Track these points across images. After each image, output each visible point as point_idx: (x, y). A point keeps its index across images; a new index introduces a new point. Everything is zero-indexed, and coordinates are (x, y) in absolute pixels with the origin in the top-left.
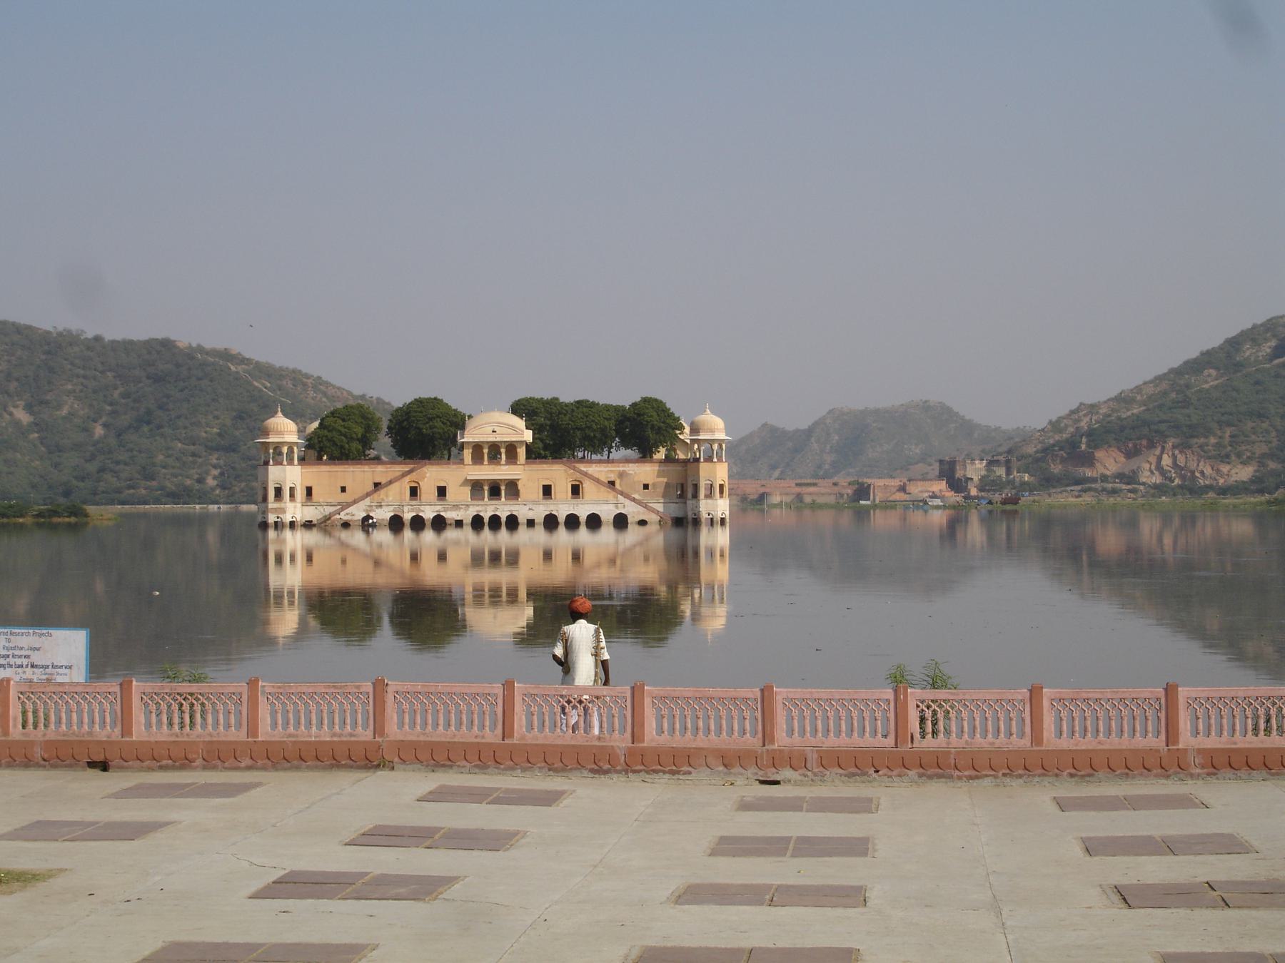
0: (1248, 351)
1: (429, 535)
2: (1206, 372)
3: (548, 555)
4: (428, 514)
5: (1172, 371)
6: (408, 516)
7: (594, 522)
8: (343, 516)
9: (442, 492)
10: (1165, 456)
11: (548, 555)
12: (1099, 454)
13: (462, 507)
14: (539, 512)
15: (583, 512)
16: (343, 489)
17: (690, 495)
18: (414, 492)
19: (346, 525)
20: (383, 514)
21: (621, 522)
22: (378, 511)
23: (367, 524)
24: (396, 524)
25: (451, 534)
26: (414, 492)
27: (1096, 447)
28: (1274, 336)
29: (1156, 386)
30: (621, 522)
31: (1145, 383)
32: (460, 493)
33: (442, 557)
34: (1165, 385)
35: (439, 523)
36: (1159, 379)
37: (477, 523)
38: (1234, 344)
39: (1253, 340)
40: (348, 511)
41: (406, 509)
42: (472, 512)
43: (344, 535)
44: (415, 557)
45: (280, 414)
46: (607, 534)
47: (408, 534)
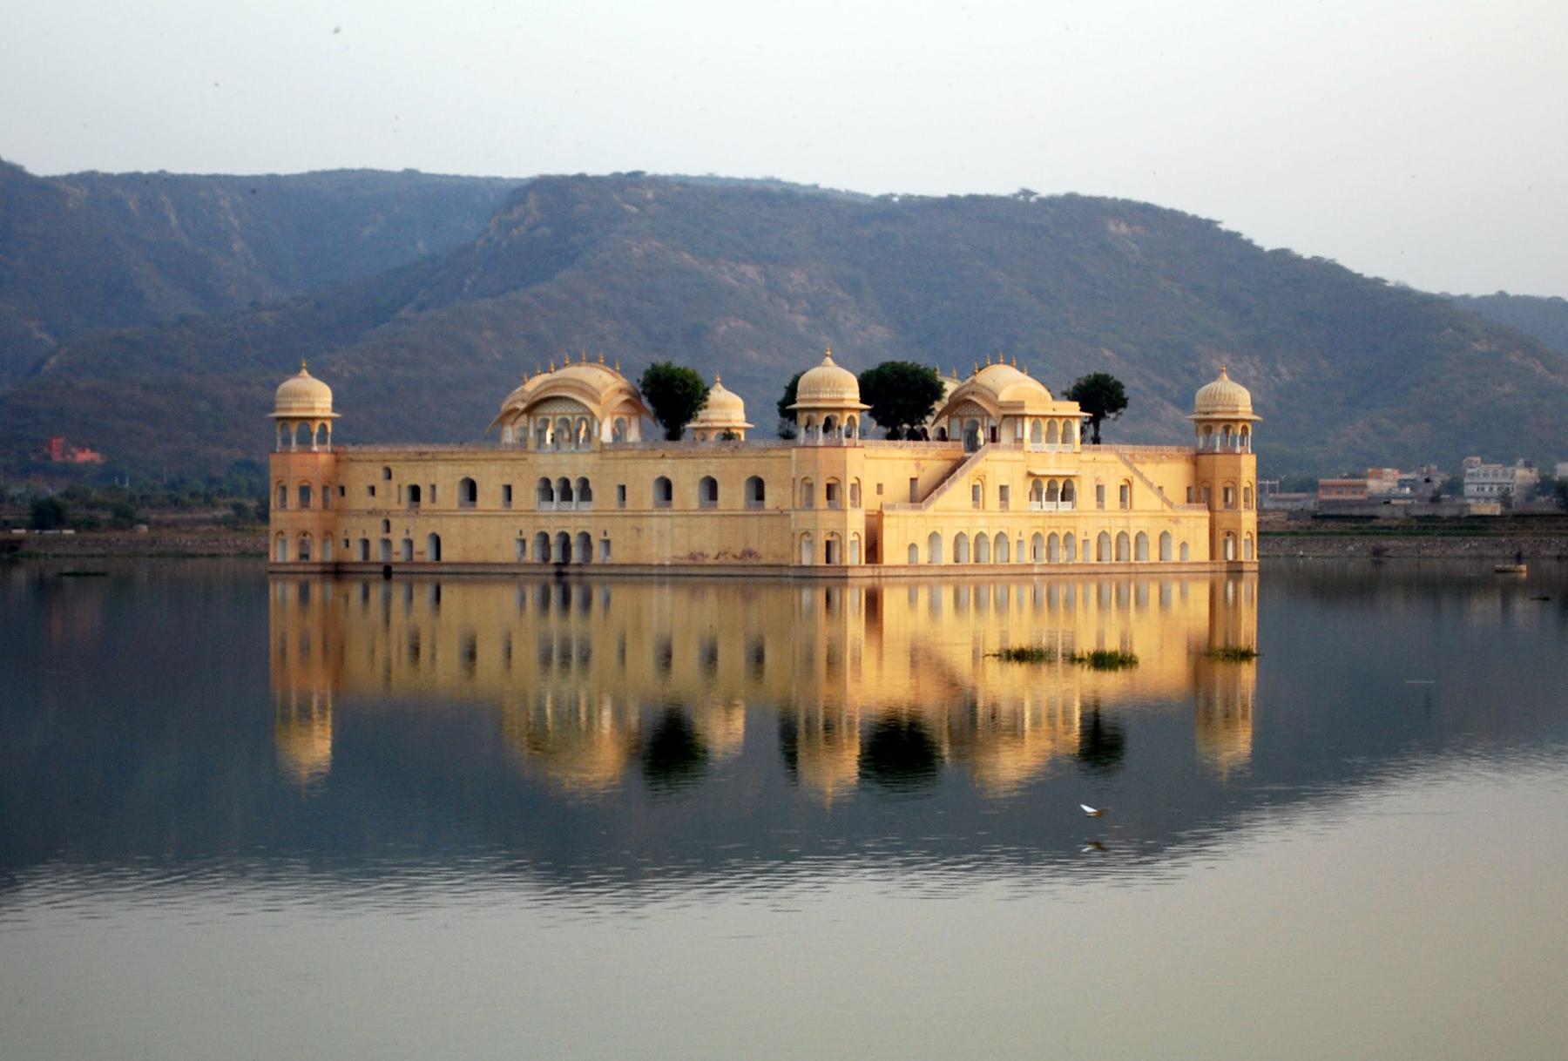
17: (1219, 503)
45: (829, 360)
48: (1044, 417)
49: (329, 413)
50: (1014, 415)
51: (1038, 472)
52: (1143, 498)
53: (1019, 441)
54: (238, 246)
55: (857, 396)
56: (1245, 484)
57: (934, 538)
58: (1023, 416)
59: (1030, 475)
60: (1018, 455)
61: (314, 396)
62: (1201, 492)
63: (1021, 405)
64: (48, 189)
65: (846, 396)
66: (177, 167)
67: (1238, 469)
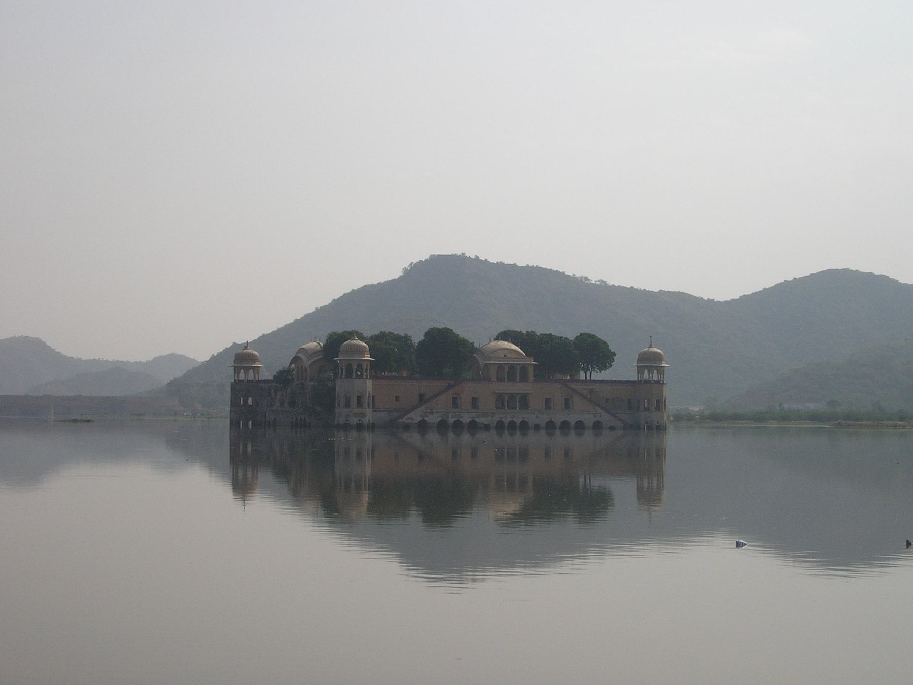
1: (466, 438)
3: (547, 454)
4: (466, 419)
5: (296, 321)
6: (451, 421)
7: (580, 426)
8: (404, 420)
11: (547, 454)
14: (543, 419)
15: (573, 419)
16: (397, 398)
18: (455, 401)
19: (407, 427)
20: (433, 419)
21: (597, 426)
22: (431, 416)
23: (423, 427)
24: (442, 427)
25: (482, 436)
26: (455, 401)
30: (597, 426)
33: (474, 453)
35: (473, 427)
37: (500, 426)
40: (409, 416)
41: (450, 415)
42: (497, 418)
43: (405, 436)
44: (454, 453)
46: (588, 437)
47: (451, 436)
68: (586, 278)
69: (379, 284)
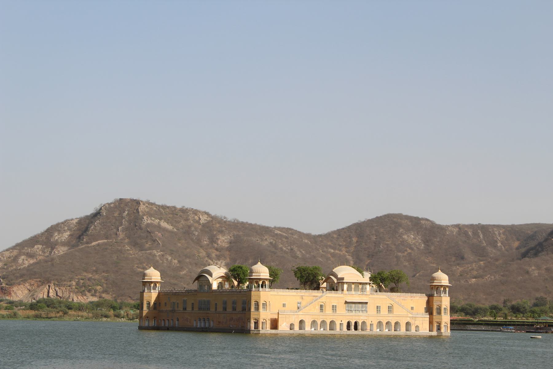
0: (56, 236)
2: (36, 247)
5: (18, 245)
9: (334, 308)
10: (51, 291)
12: (15, 289)
13: (343, 317)
16: (284, 305)
27: (11, 285)
28: (69, 229)
29: (11, 252)
31: (4, 251)
32: (342, 309)
34: (15, 252)
36: (14, 248)
38: (50, 231)
39: (59, 232)
48: (353, 283)
49: (160, 280)
50: (341, 281)
51: (348, 301)
52: (397, 310)
53: (343, 290)
54: (499, 244)
55: (268, 275)
56: (443, 307)
57: (301, 322)
58: (344, 282)
59: (346, 302)
60: (342, 296)
61: (154, 275)
62: (429, 310)
63: (343, 279)
64: (441, 229)
65: (261, 274)
66: (484, 222)
67: (441, 301)
68: (225, 218)
69: (76, 219)
